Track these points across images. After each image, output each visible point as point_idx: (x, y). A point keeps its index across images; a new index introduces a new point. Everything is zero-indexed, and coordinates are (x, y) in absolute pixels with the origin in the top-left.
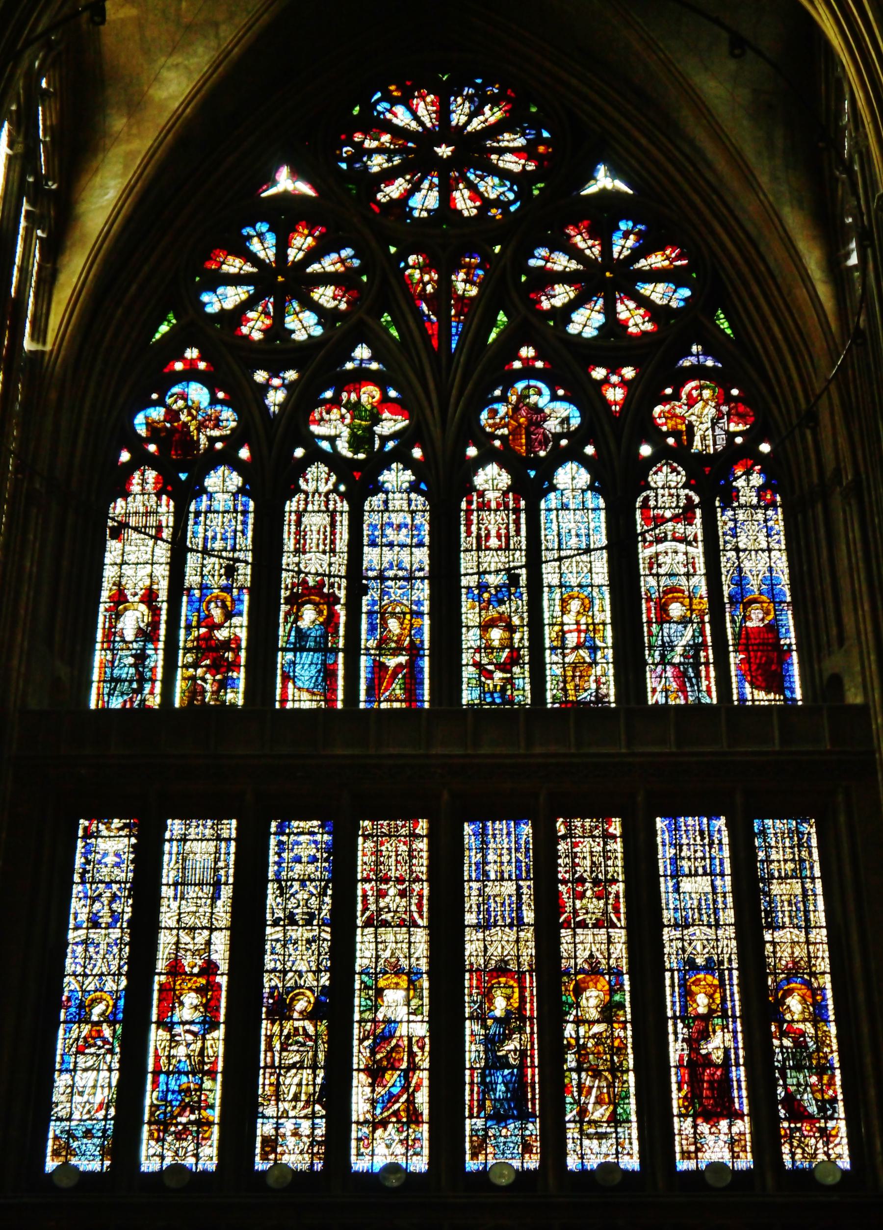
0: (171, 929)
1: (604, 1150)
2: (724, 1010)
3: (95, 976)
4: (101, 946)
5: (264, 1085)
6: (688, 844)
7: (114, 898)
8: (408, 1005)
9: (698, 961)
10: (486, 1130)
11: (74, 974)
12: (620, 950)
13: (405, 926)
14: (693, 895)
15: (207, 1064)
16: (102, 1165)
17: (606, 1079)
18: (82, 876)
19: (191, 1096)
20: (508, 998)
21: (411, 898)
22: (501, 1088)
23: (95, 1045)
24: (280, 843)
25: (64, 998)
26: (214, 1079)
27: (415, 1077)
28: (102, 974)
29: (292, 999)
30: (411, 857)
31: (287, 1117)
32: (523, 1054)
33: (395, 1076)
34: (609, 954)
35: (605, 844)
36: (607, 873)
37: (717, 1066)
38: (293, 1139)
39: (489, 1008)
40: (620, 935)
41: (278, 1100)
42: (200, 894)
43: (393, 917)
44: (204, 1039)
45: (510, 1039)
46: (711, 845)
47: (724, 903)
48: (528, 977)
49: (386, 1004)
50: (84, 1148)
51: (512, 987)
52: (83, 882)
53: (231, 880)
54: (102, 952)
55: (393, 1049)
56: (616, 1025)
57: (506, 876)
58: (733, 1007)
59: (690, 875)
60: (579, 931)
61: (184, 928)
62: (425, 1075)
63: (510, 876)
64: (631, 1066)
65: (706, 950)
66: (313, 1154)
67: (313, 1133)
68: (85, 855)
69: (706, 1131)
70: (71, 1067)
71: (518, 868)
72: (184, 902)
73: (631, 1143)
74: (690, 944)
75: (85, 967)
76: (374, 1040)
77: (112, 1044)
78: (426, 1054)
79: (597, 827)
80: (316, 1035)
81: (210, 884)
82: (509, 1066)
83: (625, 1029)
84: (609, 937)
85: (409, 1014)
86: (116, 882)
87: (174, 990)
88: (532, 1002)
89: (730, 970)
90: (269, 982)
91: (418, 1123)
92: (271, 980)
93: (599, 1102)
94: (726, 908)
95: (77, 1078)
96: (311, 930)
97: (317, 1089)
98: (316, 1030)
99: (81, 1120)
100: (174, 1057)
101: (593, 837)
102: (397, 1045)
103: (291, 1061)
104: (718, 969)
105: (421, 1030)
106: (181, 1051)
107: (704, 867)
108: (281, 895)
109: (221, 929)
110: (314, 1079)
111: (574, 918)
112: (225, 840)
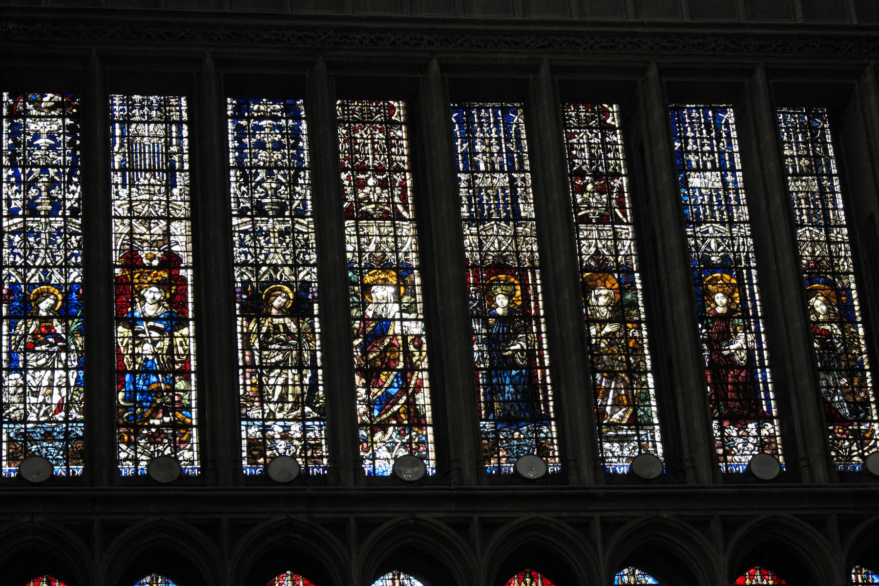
0: (122, 218)
1: (626, 452)
2: (745, 310)
3: (39, 267)
4: (43, 236)
5: (245, 385)
6: (694, 138)
7: (52, 183)
8: (399, 302)
9: (713, 259)
10: (497, 432)
11: (14, 265)
12: (627, 246)
13: (389, 219)
14: (703, 191)
15: (177, 363)
16: (68, 469)
17: (623, 380)
18: (12, 159)
19: (163, 396)
20: (510, 296)
21: (393, 189)
22: (509, 389)
23: (46, 342)
24: (239, 128)
25: (4, 292)
26: (188, 380)
27: (414, 378)
28: (46, 266)
29: (269, 295)
30: (390, 146)
31: (276, 420)
32: (530, 354)
33: (392, 377)
34: (617, 251)
35: (604, 136)
36: (608, 166)
37: (741, 368)
38: (283, 442)
39: (489, 306)
40: (627, 231)
41: (262, 402)
42: (152, 181)
43: (374, 209)
44: (172, 337)
45: (516, 338)
46: (719, 138)
47: (737, 199)
48: (529, 273)
49: (374, 300)
50: (44, 451)
51: (513, 284)
52: (14, 165)
53: (186, 166)
54: (44, 242)
55: (386, 348)
56: (629, 325)
57: (497, 167)
58: (754, 307)
59: (698, 170)
60: (582, 226)
61: (138, 218)
62: (425, 374)
63: (502, 166)
64: (649, 367)
65: (721, 248)
66: (306, 457)
67: (304, 436)
68: (10, 136)
69: (734, 434)
70: (21, 365)
71: (510, 159)
72: (134, 189)
73: (655, 446)
74: (703, 242)
75: (26, 258)
76: (365, 339)
77: (66, 341)
78: (424, 354)
79: (593, 118)
80: (299, 332)
81: (163, 171)
82: (516, 366)
83: (640, 329)
84: (615, 233)
85: (401, 311)
86: (53, 167)
87: (133, 284)
88: (536, 301)
89: (749, 269)
90: (241, 276)
91: (422, 425)
92: (242, 274)
93: (617, 404)
94: (739, 204)
95: (29, 377)
96: (284, 222)
97: (305, 390)
98: (298, 327)
99: (38, 422)
100: (139, 355)
101: (591, 128)
102: (391, 344)
103: (273, 361)
104: (736, 268)
105: (416, 328)
106: (147, 348)
107: (713, 162)
108: (246, 183)
109: (180, 219)
110: (301, 379)
111: (576, 214)
112: (175, 122)
